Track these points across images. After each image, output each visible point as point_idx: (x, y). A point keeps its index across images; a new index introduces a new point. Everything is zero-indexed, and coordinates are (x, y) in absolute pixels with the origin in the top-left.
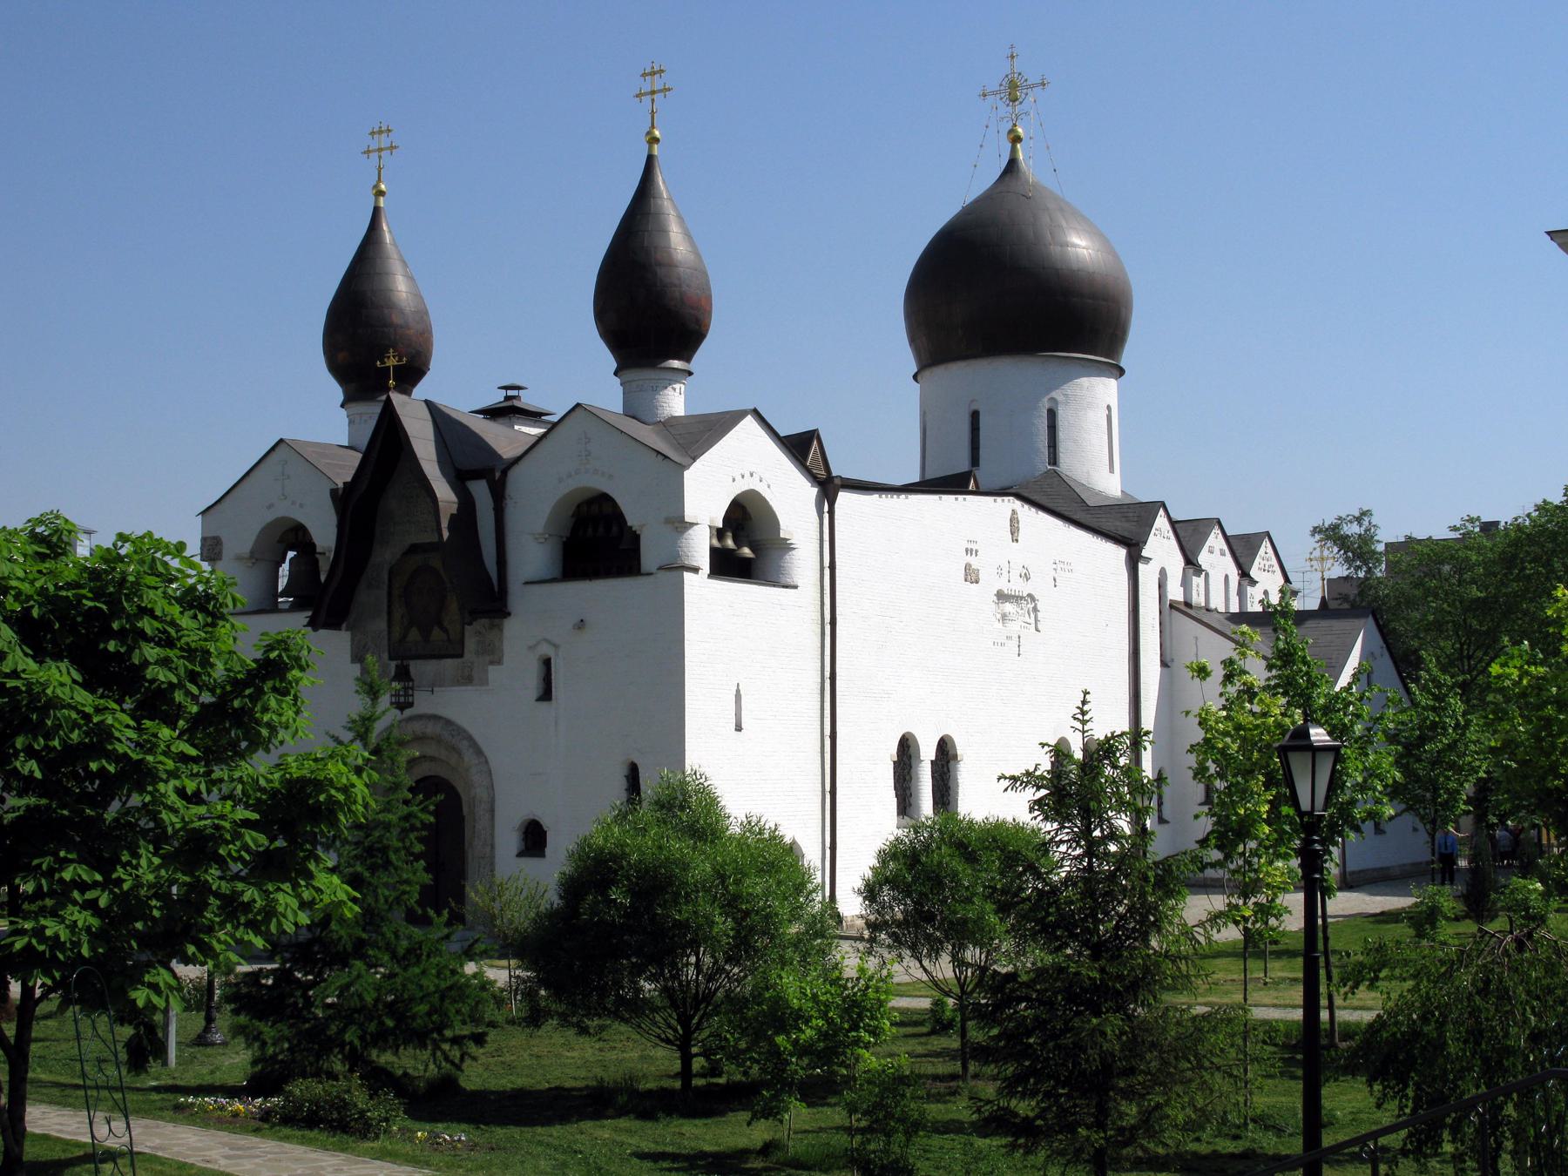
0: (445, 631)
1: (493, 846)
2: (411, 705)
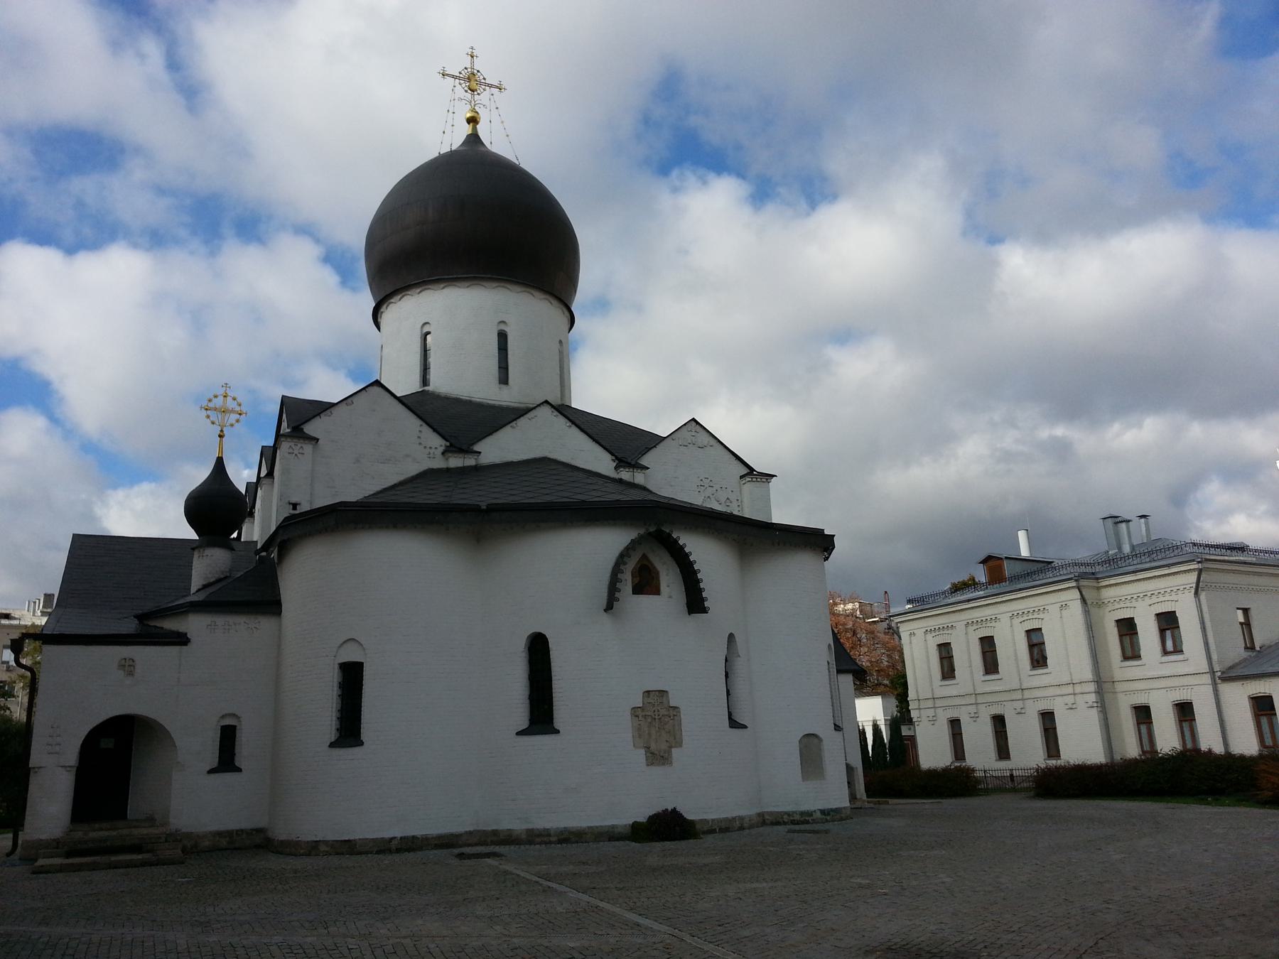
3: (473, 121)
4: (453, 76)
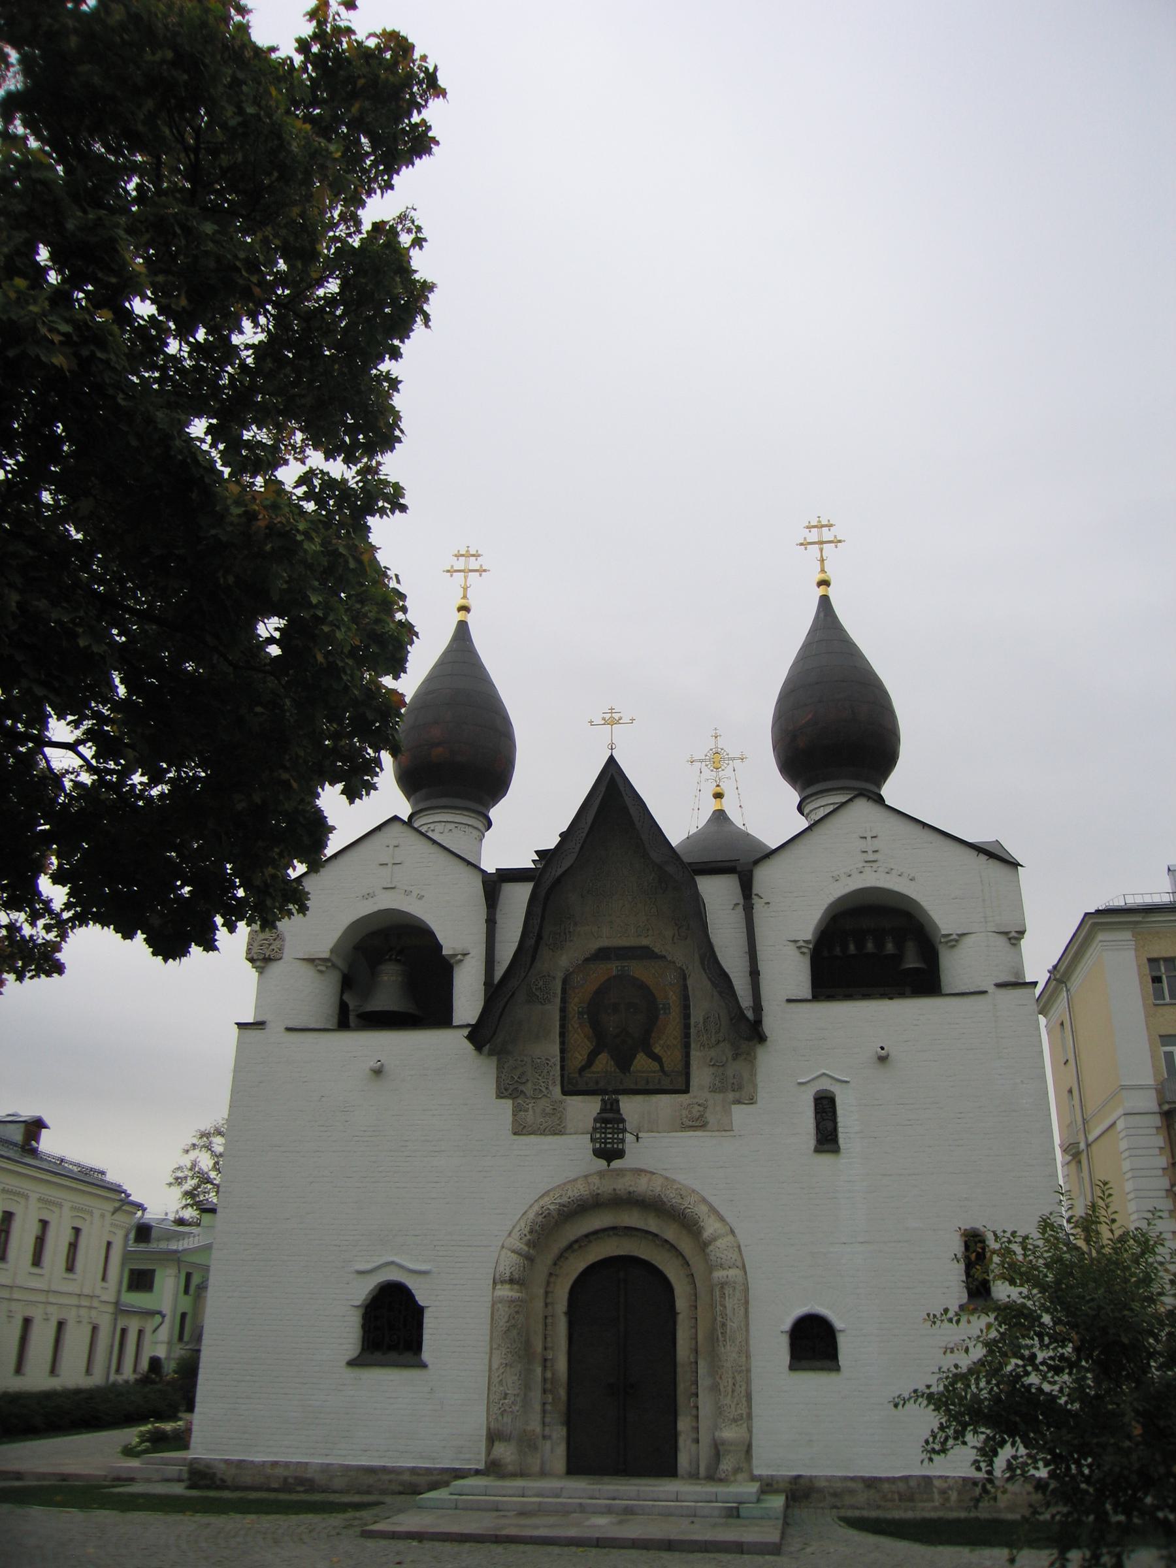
0: (656, 1058)
1: (748, 1357)
2: (620, 1154)
3: (718, 796)
4: (701, 761)
